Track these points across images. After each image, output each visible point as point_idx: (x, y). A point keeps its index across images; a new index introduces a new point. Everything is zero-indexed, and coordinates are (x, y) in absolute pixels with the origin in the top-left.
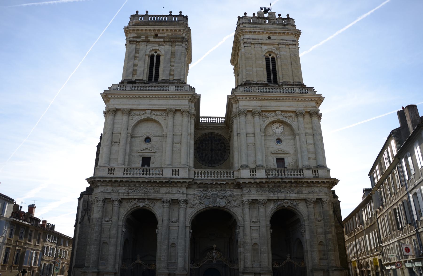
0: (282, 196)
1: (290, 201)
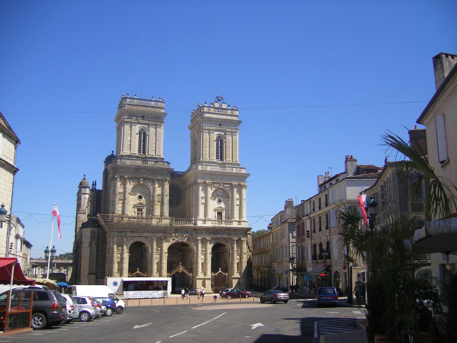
0: (219, 236)
1: (223, 240)
